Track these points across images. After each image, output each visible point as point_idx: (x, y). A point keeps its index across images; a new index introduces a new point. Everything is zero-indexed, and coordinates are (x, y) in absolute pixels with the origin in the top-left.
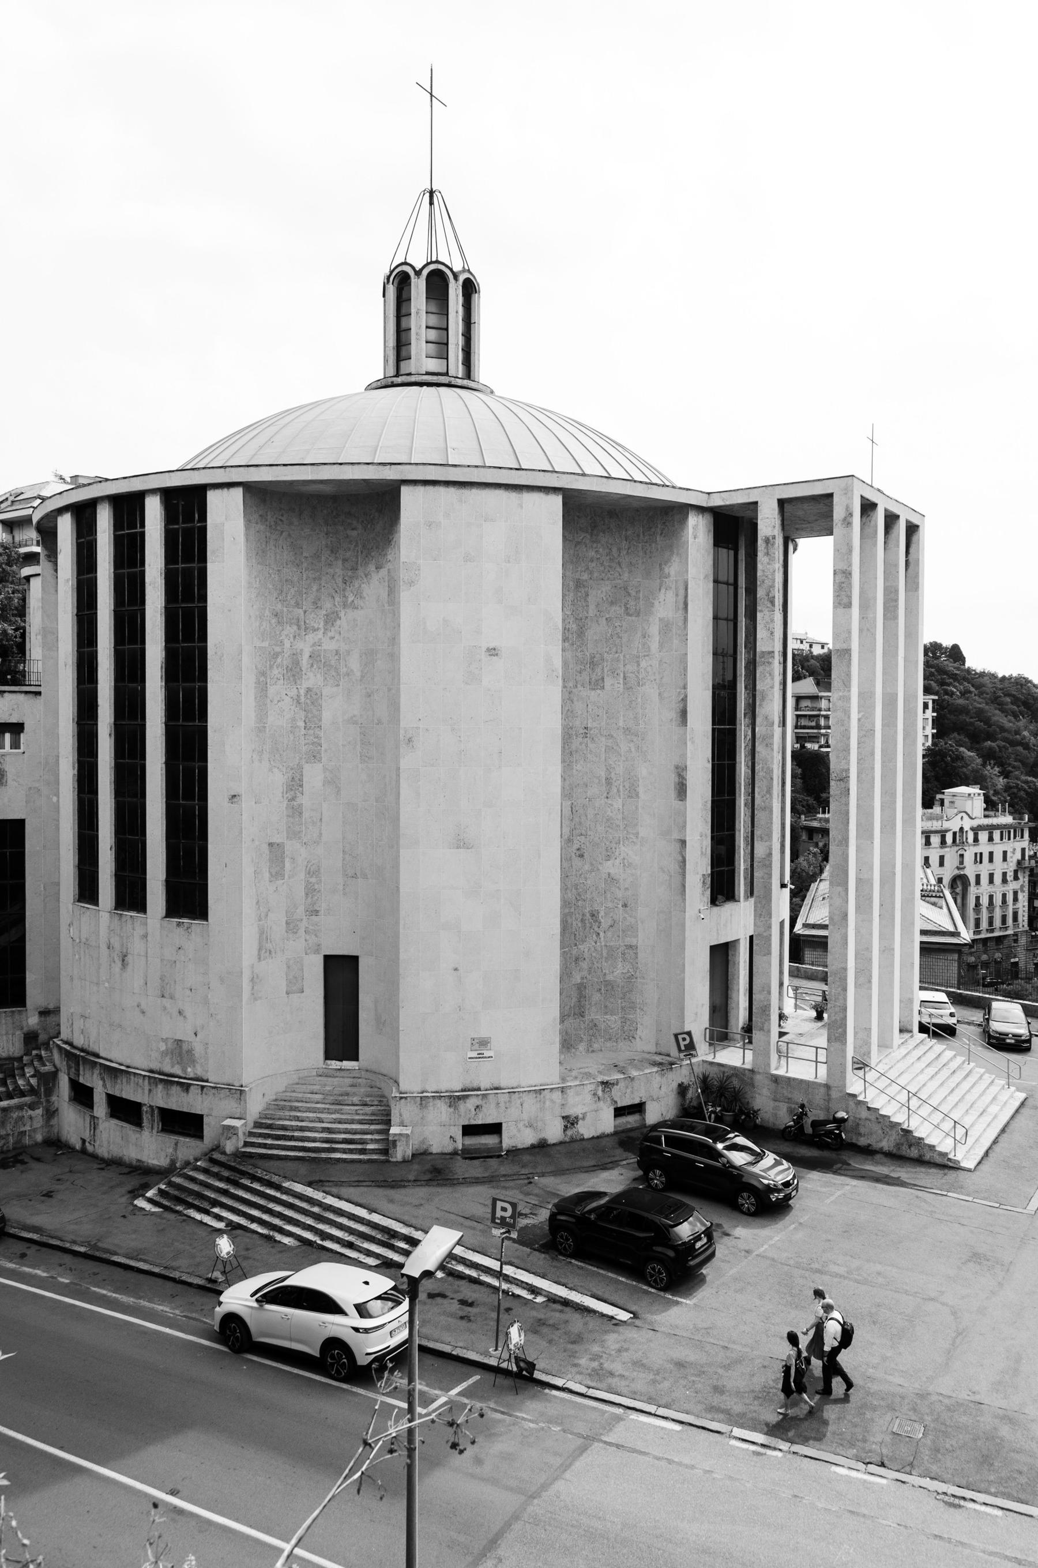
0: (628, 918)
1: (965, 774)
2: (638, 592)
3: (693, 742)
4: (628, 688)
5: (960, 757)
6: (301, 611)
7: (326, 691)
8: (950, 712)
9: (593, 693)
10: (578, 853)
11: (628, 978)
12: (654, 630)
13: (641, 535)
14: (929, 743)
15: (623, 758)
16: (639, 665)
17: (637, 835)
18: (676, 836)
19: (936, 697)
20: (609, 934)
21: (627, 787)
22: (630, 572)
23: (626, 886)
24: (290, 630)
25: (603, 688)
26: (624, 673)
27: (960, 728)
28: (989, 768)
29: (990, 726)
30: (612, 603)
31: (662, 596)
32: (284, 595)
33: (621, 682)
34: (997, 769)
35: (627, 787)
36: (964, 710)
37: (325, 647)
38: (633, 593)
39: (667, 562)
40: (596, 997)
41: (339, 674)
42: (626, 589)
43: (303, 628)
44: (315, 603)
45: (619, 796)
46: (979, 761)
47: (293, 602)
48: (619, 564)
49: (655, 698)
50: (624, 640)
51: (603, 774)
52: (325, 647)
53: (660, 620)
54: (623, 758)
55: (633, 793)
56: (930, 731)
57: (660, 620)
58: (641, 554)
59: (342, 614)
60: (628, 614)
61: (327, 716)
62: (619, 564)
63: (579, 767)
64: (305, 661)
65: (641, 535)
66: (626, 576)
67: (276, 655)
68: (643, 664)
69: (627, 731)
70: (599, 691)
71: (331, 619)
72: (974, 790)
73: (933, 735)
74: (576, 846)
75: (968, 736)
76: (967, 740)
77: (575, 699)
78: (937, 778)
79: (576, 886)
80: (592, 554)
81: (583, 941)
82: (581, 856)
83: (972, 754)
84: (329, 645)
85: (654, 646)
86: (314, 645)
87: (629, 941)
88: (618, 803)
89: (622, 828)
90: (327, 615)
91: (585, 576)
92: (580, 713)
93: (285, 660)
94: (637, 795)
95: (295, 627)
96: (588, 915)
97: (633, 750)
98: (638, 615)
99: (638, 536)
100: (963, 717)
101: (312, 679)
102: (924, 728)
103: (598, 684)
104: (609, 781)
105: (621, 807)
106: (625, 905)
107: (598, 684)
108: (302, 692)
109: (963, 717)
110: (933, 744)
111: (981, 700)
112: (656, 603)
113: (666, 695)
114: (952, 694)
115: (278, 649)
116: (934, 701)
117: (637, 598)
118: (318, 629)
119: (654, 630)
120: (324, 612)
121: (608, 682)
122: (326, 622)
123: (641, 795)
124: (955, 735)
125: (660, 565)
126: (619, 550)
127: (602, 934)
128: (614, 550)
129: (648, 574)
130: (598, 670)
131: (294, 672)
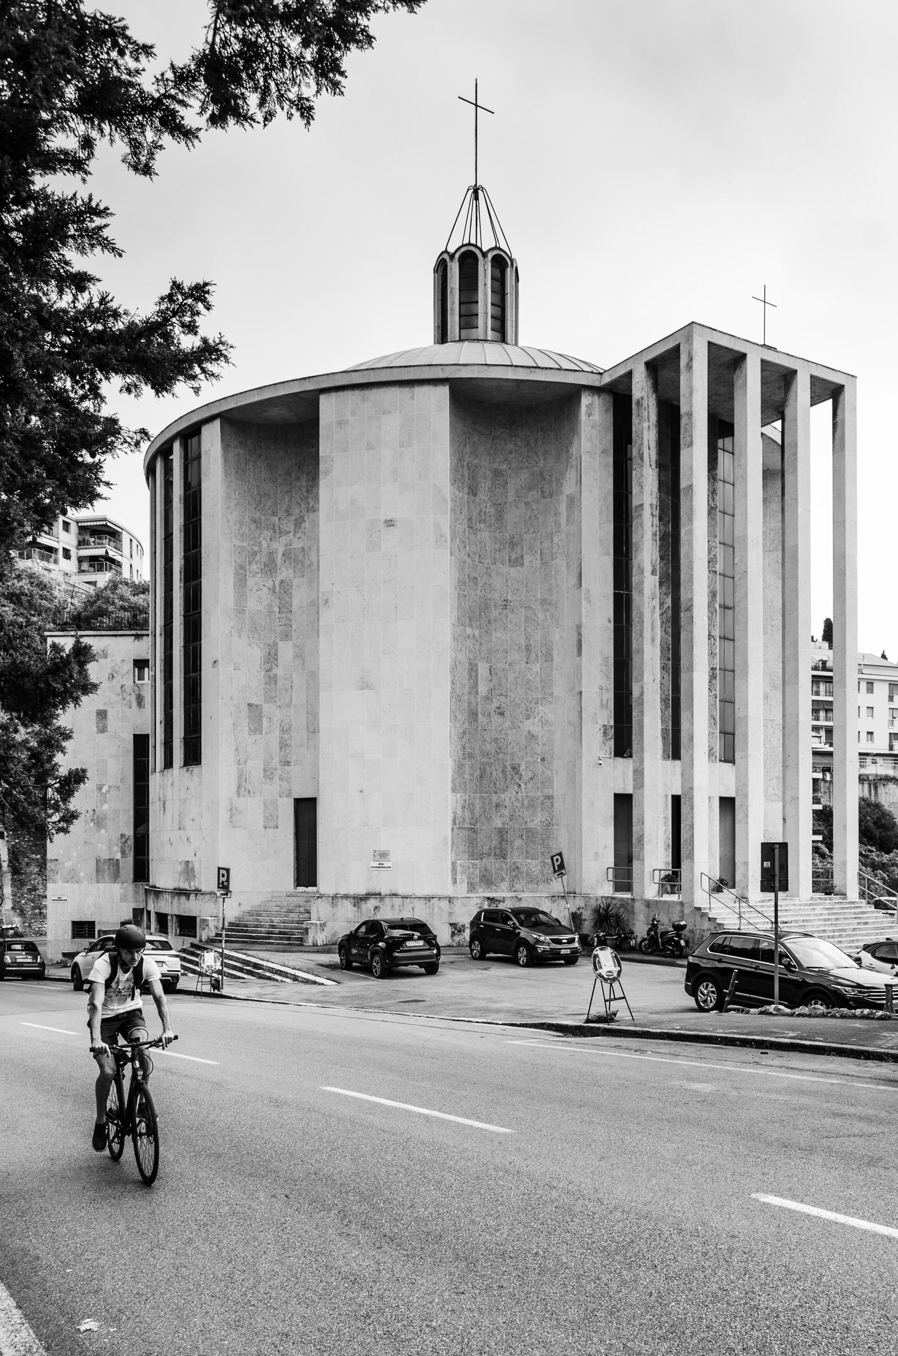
0: (546, 771)
2: (551, 476)
3: (589, 602)
4: (545, 563)
6: (276, 519)
7: (296, 582)
9: (512, 569)
10: (497, 711)
11: (547, 826)
12: (563, 508)
13: (553, 425)
15: (541, 627)
16: (552, 541)
17: (552, 694)
18: (577, 690)
20: (530, 785)
21: (544, 652)
22: (545, 459)
23: (544, 742)
24: (267, 533)
25: (522, 564)
26: (541, 550)
30: (530, 489)
31: (568, 476)
32: (262, 505)
33: (539, 558)
35: (544, 652)
37: (294, 546)
38: (548, 477)
39: (571, 443)
40: (518, 843)
41: (303, 566)
42: (541, 474)
43: (279, 532)
44: (287, 511)
45: (538, 661)
47: (269, 512)
48: (536, 453)
49: (564, 569)
50: (541, 520)
51: (522, 641)
52: (294, 546)
53: (567, 496)
54: (541, 627)
55: (549, 657)
57: (567, 496)
58: (553, 441)
59: (306, 519)
60: (544, 497)
61: (296, 602)
62: (536, 453)
63: (499, 635)
64: (279, 558)
65: (553, 425)
66: (541, 464)
67: (255, 554)
68: (555, 540)
69: (544, 602)
70: (518, 568)
71: (299, 522)
74: (495, 705)
77: (493, 574)
79: (496, 740)
80: (510, 446)
81: (504, 791)
82: (502, 714)
84: (297, 544)
85: (563, 520)
86: (286, 545)
87: (547, 792)
88: (536, 667)
89: (540, 689)
90: (296, 520)
91: (504, 467)
92: (498, 586)
93: (262, 557)
94: (552, 660)
95: (271, 531)
96: (509, 768)
97: (548, 618)
98: (551, 497)
99: (551, 425)
101: (285, 573)
103: (517, 562)
104: (528, 648)
105: (539, 670)
106: (543, 760)
107: (517, 562)
108: (277, 583)
112: (564, 482)
113: (571, 563)
115: (256, 549)
117: (550, 482)
118: (289, 532)
119: (563, 508)
120: (294, 518)
121: (527, 559)
122: (295, 526)
123: (555, 658)
125: (567, 447)
126: (536, 441)
127: (523, 786)
128: (532, 442)
129: (558, 459)
130: (518, 549)
131: (270, 567)
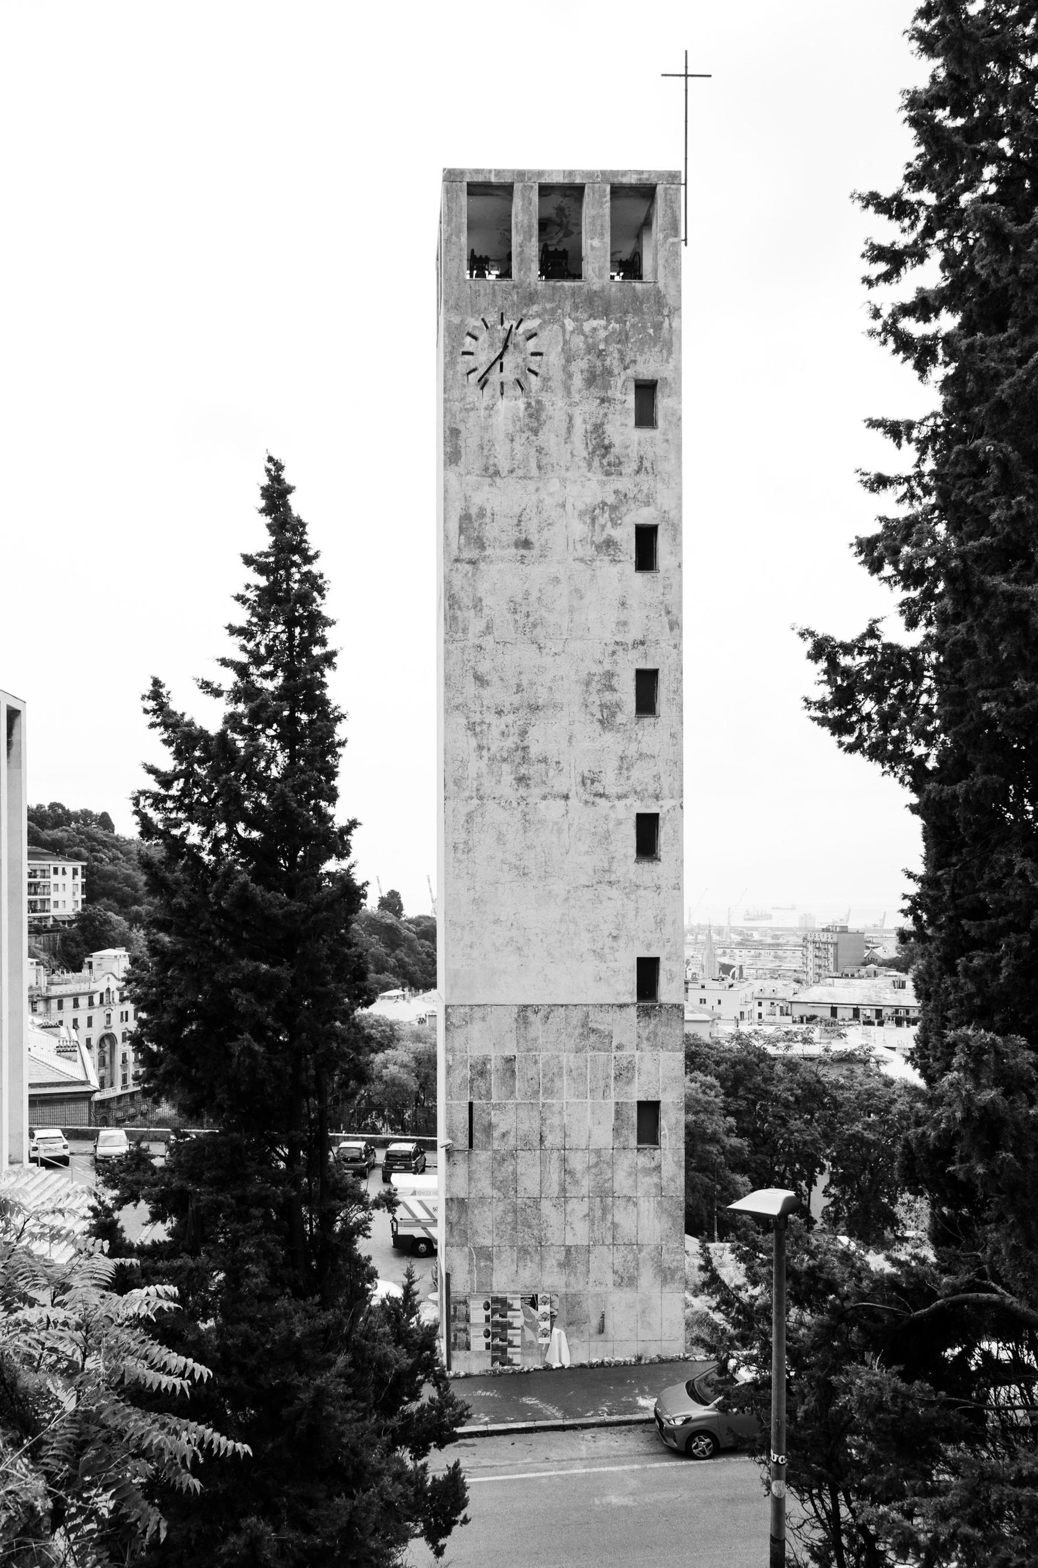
1: (113, 937)
5: (107, 922)
8: (100, 878)
14: (79, 908)
19: (85, 864)
27: (109, 893)
28: (135, 930)
29: (137, 891)
34: (142, 932)
36: (113, 876)
46: (126, 924)
56: (80, 896)
72: (121, 951)
73: (83, 901)
75: (117, 901)
76: (115, 904)
78: (86, 942)
83: (119, 918)
100: (112, 883)
102: (74, 894)
109: (112, 883)
110: (84, 909)
111: (128, 866)
114: (101, 860)
116: (83, 867)
124: (105, 900)
